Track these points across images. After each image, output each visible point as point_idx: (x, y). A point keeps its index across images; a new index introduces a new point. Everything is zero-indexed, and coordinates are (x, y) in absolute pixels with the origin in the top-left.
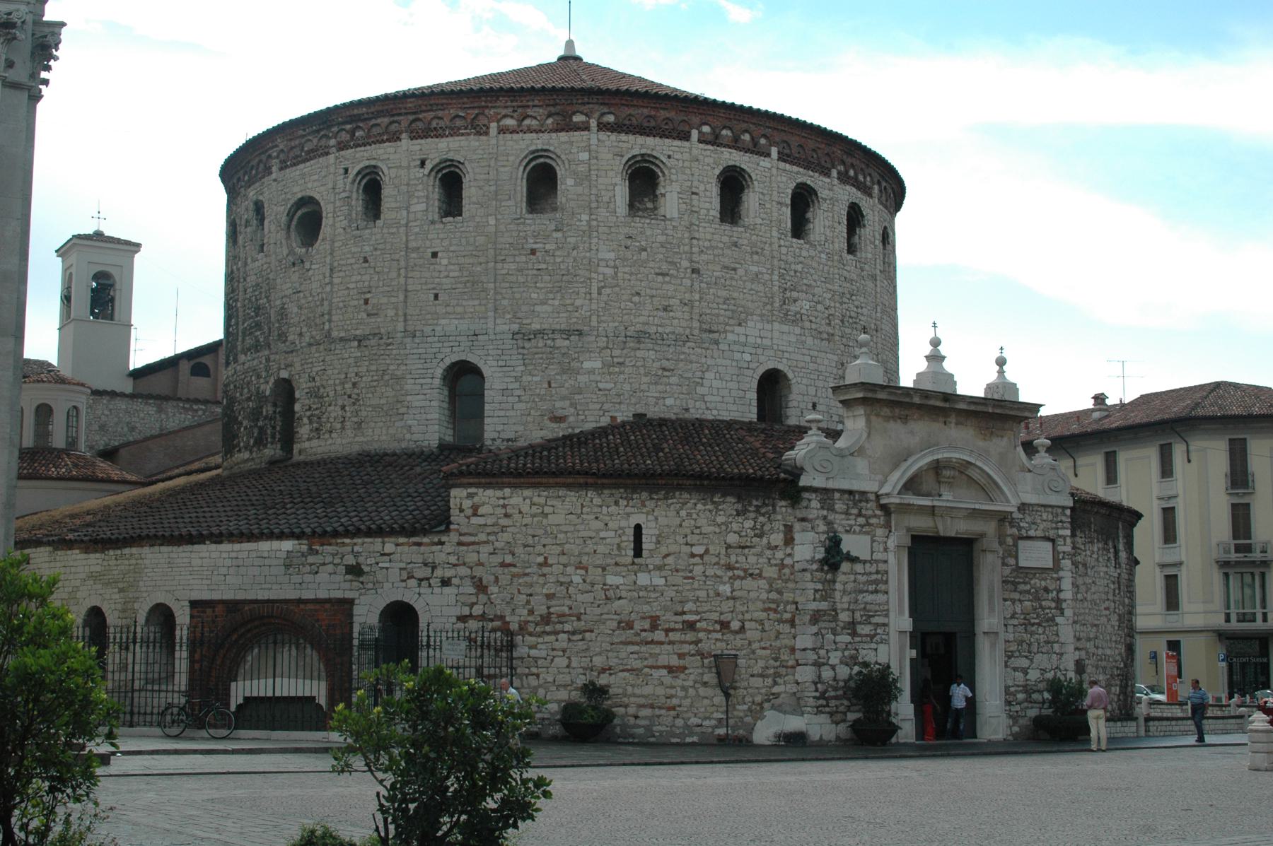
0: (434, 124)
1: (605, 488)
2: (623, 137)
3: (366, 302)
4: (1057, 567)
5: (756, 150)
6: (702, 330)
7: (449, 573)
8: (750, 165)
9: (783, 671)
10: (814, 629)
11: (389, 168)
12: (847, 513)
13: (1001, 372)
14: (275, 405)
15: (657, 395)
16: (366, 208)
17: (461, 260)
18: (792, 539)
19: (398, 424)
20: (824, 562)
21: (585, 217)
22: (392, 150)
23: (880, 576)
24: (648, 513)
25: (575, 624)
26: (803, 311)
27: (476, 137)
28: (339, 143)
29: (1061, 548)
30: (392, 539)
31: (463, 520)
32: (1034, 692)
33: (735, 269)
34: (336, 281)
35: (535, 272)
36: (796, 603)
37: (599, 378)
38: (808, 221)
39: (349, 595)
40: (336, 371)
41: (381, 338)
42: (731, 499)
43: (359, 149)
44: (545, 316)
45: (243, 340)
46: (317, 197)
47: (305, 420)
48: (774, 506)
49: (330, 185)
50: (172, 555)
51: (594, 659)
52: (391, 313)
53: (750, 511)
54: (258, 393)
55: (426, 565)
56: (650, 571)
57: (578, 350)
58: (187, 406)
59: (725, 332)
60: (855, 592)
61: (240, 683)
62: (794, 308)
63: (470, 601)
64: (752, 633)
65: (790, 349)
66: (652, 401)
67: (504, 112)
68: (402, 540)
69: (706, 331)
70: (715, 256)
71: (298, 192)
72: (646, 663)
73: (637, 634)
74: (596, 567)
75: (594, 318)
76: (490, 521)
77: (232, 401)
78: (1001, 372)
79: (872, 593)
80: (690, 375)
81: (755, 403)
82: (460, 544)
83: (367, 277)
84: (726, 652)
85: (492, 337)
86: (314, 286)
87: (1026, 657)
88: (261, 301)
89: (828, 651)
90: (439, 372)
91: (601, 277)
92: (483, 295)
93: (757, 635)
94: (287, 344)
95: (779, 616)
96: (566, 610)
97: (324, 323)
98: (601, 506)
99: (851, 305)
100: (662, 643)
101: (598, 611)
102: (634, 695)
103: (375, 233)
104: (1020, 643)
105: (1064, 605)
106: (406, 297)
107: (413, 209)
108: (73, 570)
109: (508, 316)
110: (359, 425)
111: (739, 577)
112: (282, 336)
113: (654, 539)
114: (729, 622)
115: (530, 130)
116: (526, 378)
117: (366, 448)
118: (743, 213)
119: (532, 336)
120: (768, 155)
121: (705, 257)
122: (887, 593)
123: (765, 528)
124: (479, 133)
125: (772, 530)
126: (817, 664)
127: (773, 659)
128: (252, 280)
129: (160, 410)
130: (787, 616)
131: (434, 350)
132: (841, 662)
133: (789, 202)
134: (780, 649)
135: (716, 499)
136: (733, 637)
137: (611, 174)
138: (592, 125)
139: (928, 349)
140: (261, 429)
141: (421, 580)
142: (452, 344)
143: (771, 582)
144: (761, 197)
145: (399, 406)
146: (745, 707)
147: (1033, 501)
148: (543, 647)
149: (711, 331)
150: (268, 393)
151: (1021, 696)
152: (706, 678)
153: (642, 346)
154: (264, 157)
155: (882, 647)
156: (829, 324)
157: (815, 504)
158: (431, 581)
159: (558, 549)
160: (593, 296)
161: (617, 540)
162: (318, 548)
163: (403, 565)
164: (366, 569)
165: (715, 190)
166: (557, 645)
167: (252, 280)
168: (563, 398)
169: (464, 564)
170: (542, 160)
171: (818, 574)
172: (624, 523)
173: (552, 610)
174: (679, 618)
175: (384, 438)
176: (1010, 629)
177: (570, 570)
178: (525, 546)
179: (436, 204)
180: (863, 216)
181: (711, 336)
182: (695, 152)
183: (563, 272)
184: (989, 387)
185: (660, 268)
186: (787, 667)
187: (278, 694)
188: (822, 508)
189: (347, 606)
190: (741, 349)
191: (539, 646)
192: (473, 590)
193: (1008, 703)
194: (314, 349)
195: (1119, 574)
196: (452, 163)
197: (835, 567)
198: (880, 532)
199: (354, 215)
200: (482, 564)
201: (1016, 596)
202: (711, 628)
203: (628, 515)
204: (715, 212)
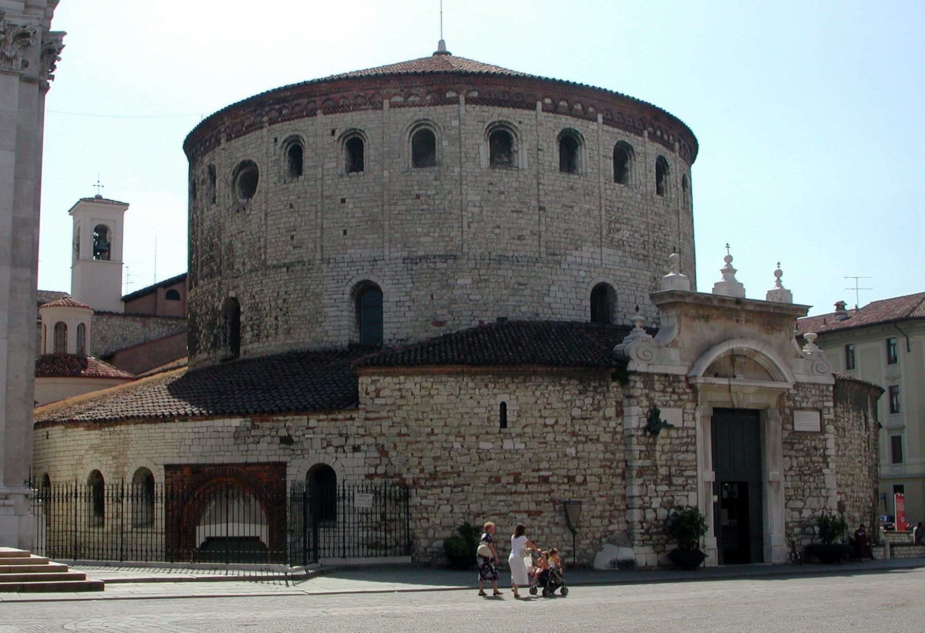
0: (341, 102)
1: (478, 375)
2: (485, 108)
3: (292, 237)
4: (823, 431)
5: (585, 116)
6: (548, 254)
7: (359, 442)
8: (582, 128)
9: (616, 513)
10: (640, 481)
11: (308, 137)
12: (664, 391)
13: (779, 282)
14: (226, 317)
15: (515, 303)
16: (292, 167)
17: (364, 204)
18: (622, 412)
19: (319, 329)
20: (646, 429)
21: (457, 170)
22: (310, 123)
23: (689, 440)
24: (510, 394)
25: (456, 479)
26: (625, 238)
27: (373, 111)
28: (270, 119)
29: (826, 416)
30: (316, 417)
31: (369, 402)
32: (807, 526)
33: (572, 207)
34: (269, 222)
35: (420, 212)
36: (626, 461)
37: (469, 292)
38: (626, 170)
39: (282, 459)
40: (271, 291)
41: (304, 265)
42: (573, 382)
43: (285, 123)
44: (428, 244)
45: (201, 271)
46: (254, 160)
47: (248, 328)
48: (608, 386)
49: (264, 151)
50: (150, 431)
51: (471, 506)
52: (311, 246)
53: (589, 391)
54: (213, 308)
55: (341, 435)
56: (513, 439)
57: (453, 270)
58: (164, 322)
59: (565, 254)
60: (671, 451)
61: (202, 527)
62: (617, 236)
63: (375, 463)
64: (592, 484)
65: (615, 267)
66: (510, 309)
67: (394, 91)
68: (322, 417)
69: (550, 254)
70: (556, 197)
71: (240, 157)
72: (511, 509)
73: (504, 487)
74: (472, 435)
75: (465, 246)
76: (390, 401)
77: (194, 315)
78: (779, 282)
79: (684, 452)
80: (539, 288)
81: (589, 309)
82: (367, 419)
83: (292, 219)
84: (572, 499)
85: (388, 262)
86: (254, 226)
87: (801, 500)
88: (214, 240)
89: (651, 498)
90: (348, 290)
91: (470, 215)
92: (380, 230)
93: (597, 486)
94: (234, 271)
95: (613, 471)
96: (449, 469)
97: (261, 255)
98: (473, 389)
99: (660, 234)
100: (523, 493)
101: (473, 469)
102: (503, 533)
103: (298, 185)
104: (796, 489)
105: (829, 460)
106: (322, 233)
107: (326, 167)
108: (79, 442)
109: (399, 246)
110: (288, 332)
111: (581, 442)
112: (231, 266)
113: (516, 413)
114: (574, 477)
115: (414, 105)
116: (414, 293)
117: (295, 348)
118: (578, 164)
119: (418, 261)
120: (596, 120)
121: (549, 198)
122: (695, 452)
123: (601, 403)
124: (375, 108)
125: (606, 406)
126: (643, 508)
127: (608, 504)
128: (207, 224)
129: (144, 326)
130: (619, 471)
131: (344, 273)
132: (661, 506)
133: (612, 156)
134: (614, 496)
135: (563, 382)
136: (577, 488)
137: (477, 136)
138: (461, 99)
139: (723, 265)
140: (215, 336)
141: (337, 447)
142: (357, 268)
143: (606, 445)
144: (591, 152)
145: (318, 316)
146: (588, 541)
147: (804, 381)
148: (432, 497)
149: (555, 255)
150: (220, 308)
151: (797, 530)
152: (557, 520)
153: (502, 266)
154: (215, 132)
155: (692, 495)
156: (644, 248)
157: (640, 385)
158: (345, 448)
159: (442, 423)
160: (464, 229)
161: (486, 415)
162: (259, 424)
163: (324, 436)
164: (295, 439)
165: (555, 147)
166: (442, 496)
167: (207, 224)
168: (443, 307)
169: (370, 434)
170: (423, 127)
171: (643, 439)
172: (492, 402)
173: (437, 469)
174: (536, 474)
175: (307, 340)
176: (789, 479)
177: (451, 438)
178: (416, 420)
179: (344, 162)
180: (668, 166)
181: (555, 258)
182: (539, 118)
183: (441, 211)
184: (770, 293)
185: (514, 207)
186: (619, 510)
187: (230, 535)
188: (645, 388)
189: (282, 468)
190: (578, 268)
191: (428, 497)
192: (377, 455)
193: (788, 535)
194: (253, 274)
195: (869, 436)
196: (354, 131)
197: (655, 433)
198: (689, 406)
199: (282, 173)
200: (384, 435)
201: (793, 453)
202: (561, 481)
203: (495, 395)
204: (556, 164)
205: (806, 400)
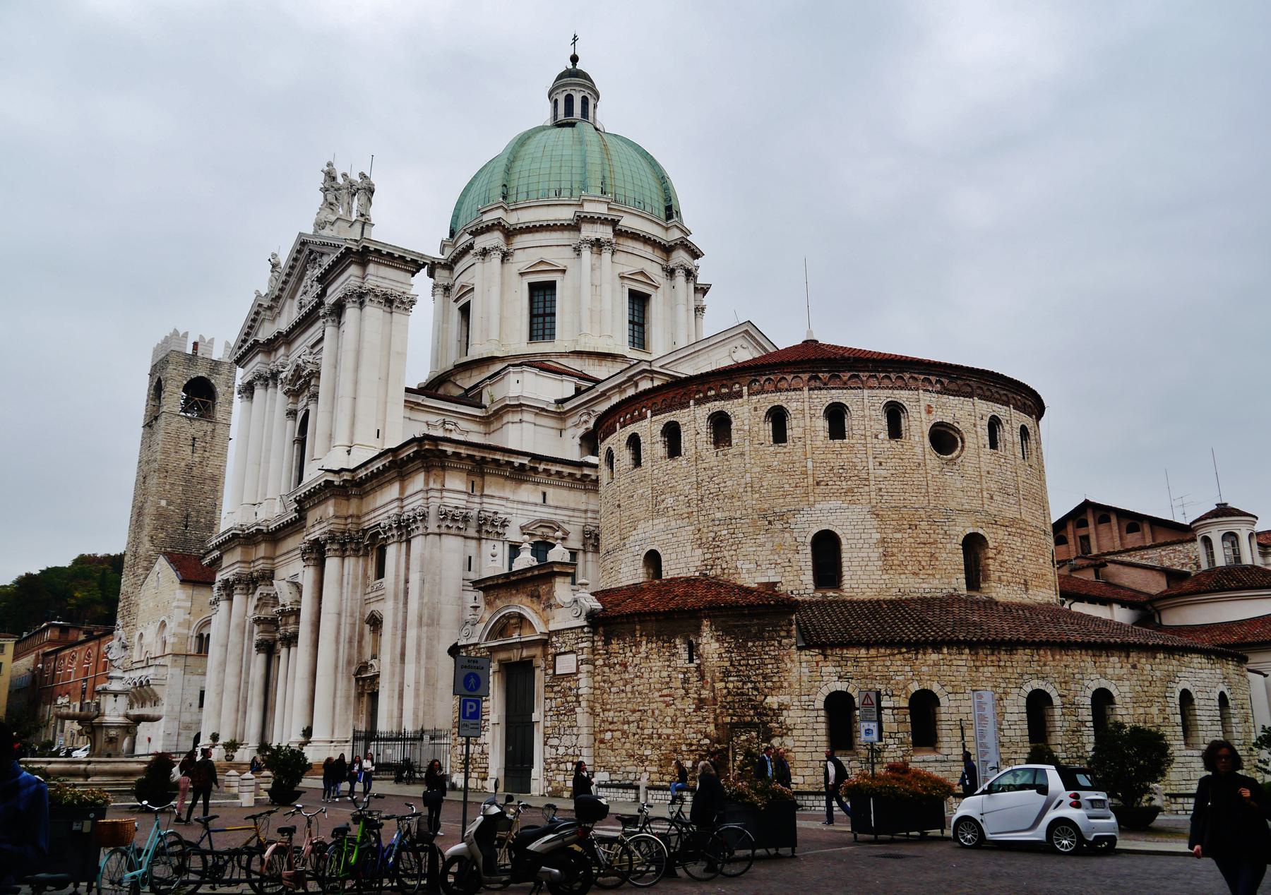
4: (578, 672)
105: (581, 699)
176: (549, 718)
193: (546, 770)
201: (552, 695)
205: (564, 645)
